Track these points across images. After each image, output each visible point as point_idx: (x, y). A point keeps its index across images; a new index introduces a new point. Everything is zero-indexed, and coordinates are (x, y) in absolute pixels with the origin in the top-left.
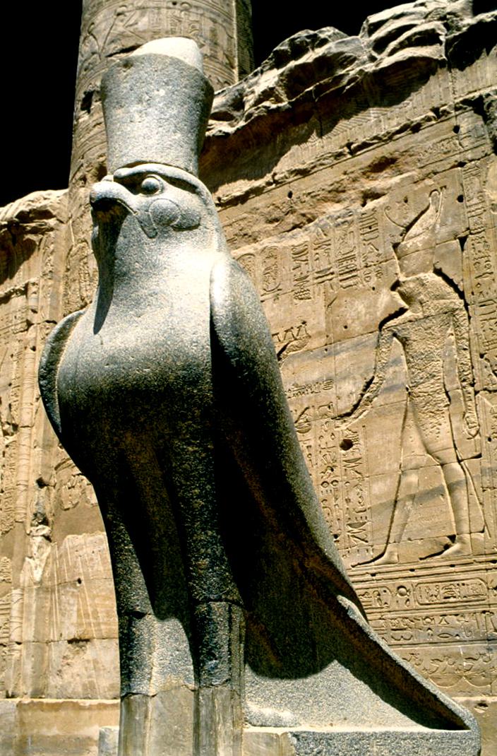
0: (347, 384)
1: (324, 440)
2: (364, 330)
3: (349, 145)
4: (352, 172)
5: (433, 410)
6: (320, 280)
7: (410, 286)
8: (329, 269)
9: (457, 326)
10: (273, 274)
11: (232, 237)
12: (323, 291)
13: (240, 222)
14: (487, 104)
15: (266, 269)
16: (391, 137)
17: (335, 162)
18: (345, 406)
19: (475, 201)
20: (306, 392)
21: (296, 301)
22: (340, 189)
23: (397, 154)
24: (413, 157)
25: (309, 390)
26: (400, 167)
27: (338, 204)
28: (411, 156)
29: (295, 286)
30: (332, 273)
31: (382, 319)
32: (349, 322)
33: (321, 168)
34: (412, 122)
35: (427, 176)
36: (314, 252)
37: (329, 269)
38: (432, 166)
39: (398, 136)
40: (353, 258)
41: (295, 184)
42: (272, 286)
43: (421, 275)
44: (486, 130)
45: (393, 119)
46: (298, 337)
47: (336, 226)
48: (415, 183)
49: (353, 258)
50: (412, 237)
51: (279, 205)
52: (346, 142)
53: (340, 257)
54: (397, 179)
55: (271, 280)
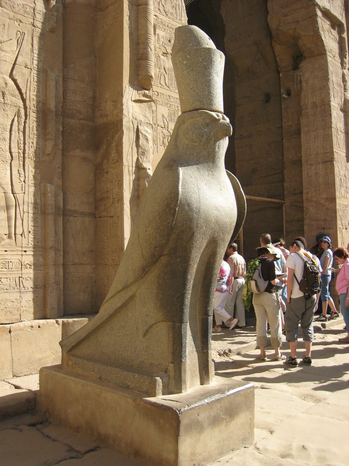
5: (3, 160)
48: (10, 19)
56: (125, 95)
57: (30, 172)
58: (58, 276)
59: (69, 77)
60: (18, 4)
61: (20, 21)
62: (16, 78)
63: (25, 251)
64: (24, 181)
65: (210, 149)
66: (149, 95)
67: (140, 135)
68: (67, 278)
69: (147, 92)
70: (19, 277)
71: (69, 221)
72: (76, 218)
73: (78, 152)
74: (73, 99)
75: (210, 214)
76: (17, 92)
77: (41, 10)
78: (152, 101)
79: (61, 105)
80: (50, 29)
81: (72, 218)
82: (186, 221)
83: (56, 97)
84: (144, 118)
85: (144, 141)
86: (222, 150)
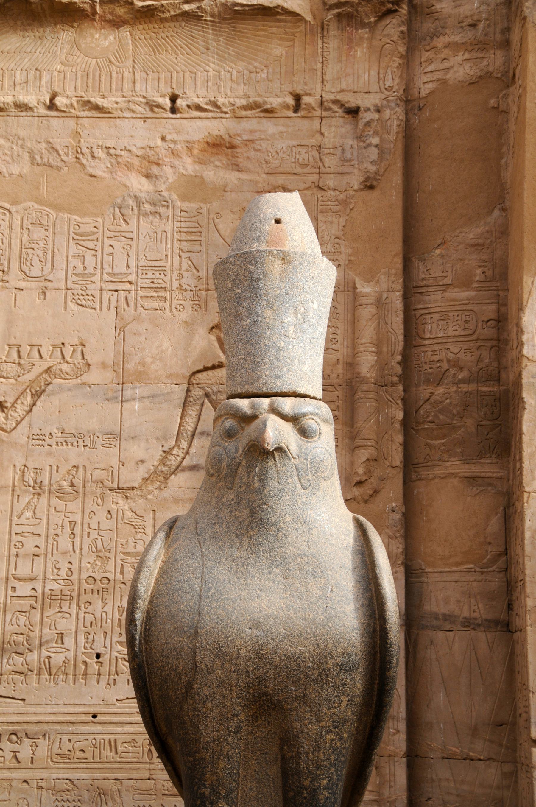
0: (136, 447)
1: (95, 520)
2: (166, 377)
3: (174, 99)
4: (174, 142)
6: (113, 286)
8: (127, 275)
12: (114, 303)
14: (365, 120)
17: (150, 114)
18: (133, 476)
20: (75, 444)
21: (71, 305)
22: (152, 158)
23: (237, 141)
24: (258, 153)
25: (81, 441)
26: (239, 160)
27: (144, 180)
28: (255, 150)
29: (73, 282)
30: (131, 283)
31: (195, 370)
32: (149, 360)
34: (265, 102)
36: (107, 242)
37: (127, 275)
38: (283, 177)
39: (244, 113)
40: (162, 270)
42: (36, 271)
44: (355, 154)
46: (69, 360)
47: (143, 215)
49: (162, 270)
51: (58, 148)
52: (170, 91)
53: (143, 263)
54: (232, 177)
56: (529, 305)
58: (391, 787)
59: (431, 282)
60: (279, 151)
65: (240, 487)
68: (430, 796)
71: (432, 642)
73: (455, 466)
75: (231, 638)
77: (338, 145)
79: (399, 358)
80: (361, 183)
81: (440, 635)
82: (168, 658)
83: (378, 344)
86: (276, 484)
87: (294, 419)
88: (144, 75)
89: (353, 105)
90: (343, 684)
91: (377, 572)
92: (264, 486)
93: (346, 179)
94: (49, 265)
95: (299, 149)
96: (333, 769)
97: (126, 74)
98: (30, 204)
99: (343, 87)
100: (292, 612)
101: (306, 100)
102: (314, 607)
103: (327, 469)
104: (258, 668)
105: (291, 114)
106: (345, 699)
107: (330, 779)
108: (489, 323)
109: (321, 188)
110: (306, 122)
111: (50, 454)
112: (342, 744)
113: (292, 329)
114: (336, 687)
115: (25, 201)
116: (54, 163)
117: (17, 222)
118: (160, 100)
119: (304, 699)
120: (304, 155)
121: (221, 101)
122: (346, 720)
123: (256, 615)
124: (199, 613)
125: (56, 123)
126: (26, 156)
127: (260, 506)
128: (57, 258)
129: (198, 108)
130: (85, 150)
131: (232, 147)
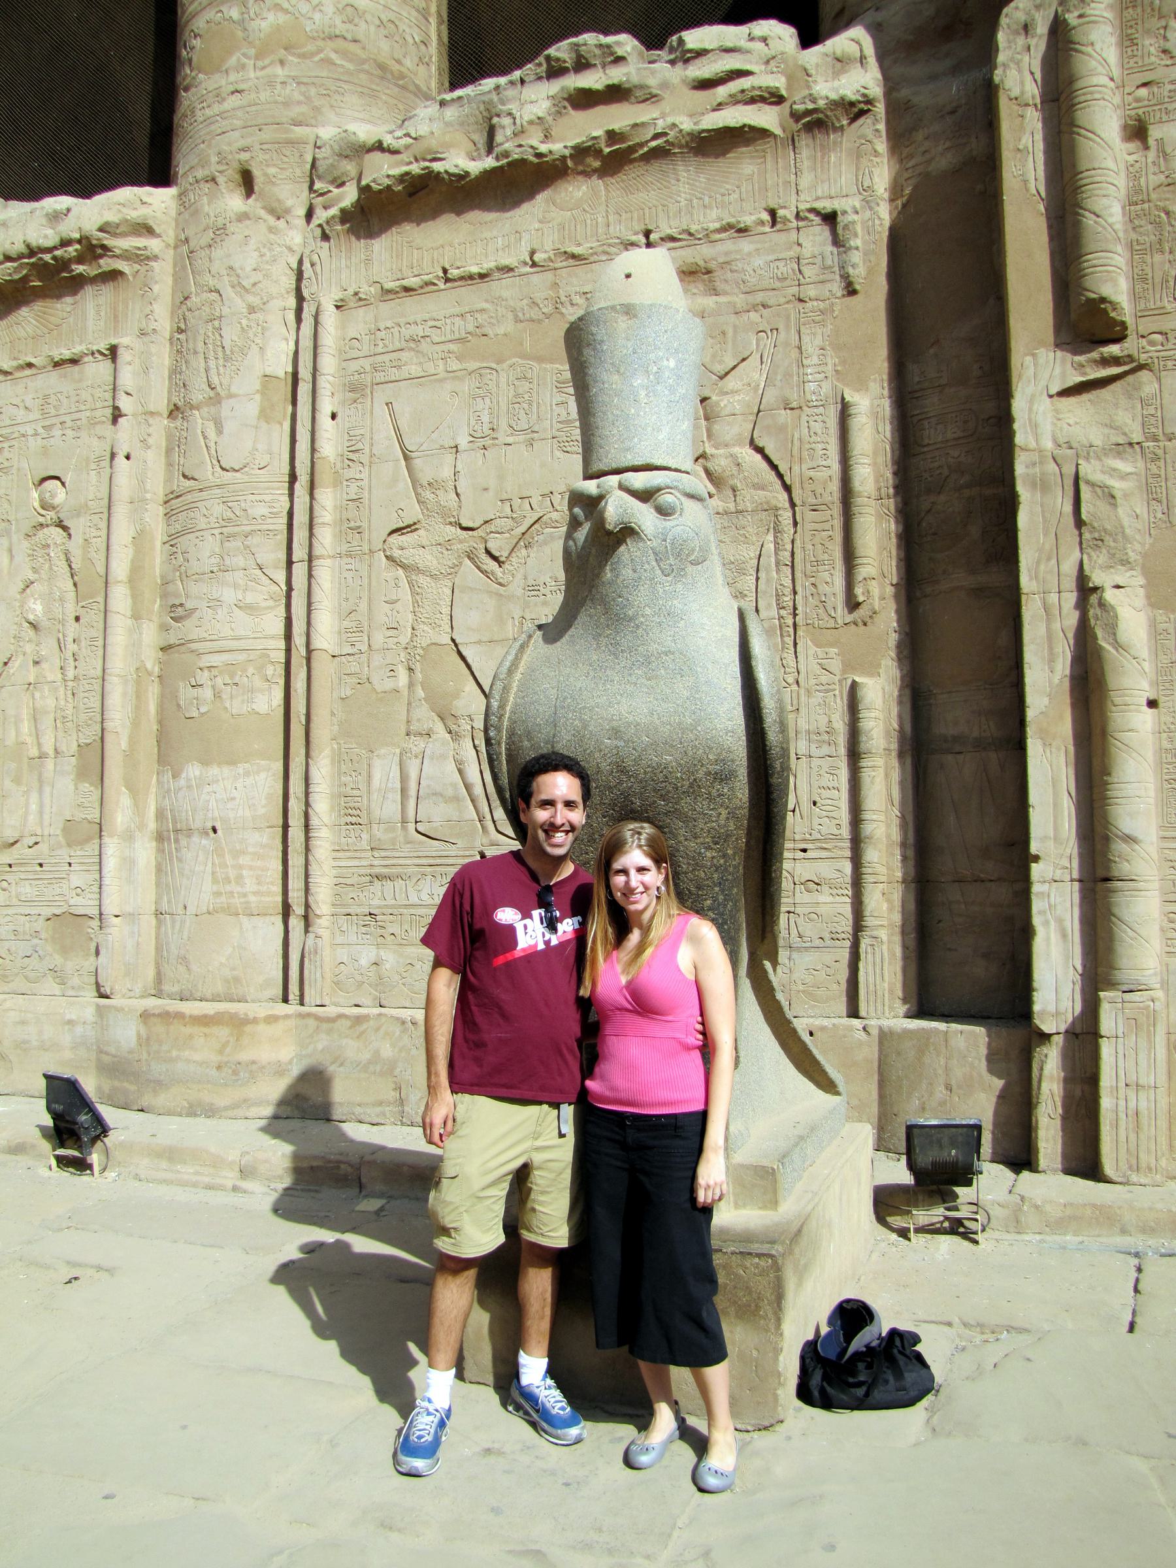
3: (647, 233)
7: (720, 463)
9: (777, 531)
10: (526, 406)
11: (464, 335)
13: (478, 315)
15: (515, 396)
16: (707, 236)
19: (815, 360)
21: (558, 454)
23: (712, 265)
28: (731, 271)
33: (604, 258)
35: (754, 308)
38: (761, 294)
39: (718, 236)
41: (564, 272)
43: (736, 450)
44: (836, 260)
45: (711, 208)
46: (559, 508)
50: (727, 393)
51: (539, 302)
52: (643, 227)
55: (522, 414)
57: (811, 658)
61: (763, 306)
62: (761, 445)
63: (804, 851)
64: (797, 682)
66: (1126, 353)
67: (1083, 488)
69: (1114, 349)
70: (789, 912)
72: (960, 757)
74: (940, 439)
76: (771, 476)
78: (1141, 367)
81: (950, 758)
84: (1106, 431)
85: (1098, 503)
86: (630, 572)
87: (645, 496)
88: (617, 216)
89: (829, 210)
90: (719, 795)
91: (754, 663)
92: (617, 576)
93: (828, 286)
94: (535, 416)
95: (777, 263)
96: (717, 889)
97: (600, 220)
98: (514, 360)
99: (820, 194)
100: (655, 717)
101: (781, 213)
102: (680, 709)
103: (693, 551)
104: (621, 782)
105: (767, 229)
106: (724, 812)
107: (715, 900)
108: (992, 420)
109: (801, 300)
110: (783, 235)
111: (545, 603)
112: (726, 862)
113: (643, 393)
114: (711, 799)
115: (510, 358)
116: (534, 317)
117: (503, 380)
118: (634, 238)
119: (677, 813)
120: (784, 269)
121: (694, 228)
122: (728, 836)
123: (615, 724)
124: (555, 726)
125: (535, 279)
126: (510, 316)
127: (614, 600)
128: (543, 408)
129: (673, 239)
130: (563, 299)
131: (708, 272)
